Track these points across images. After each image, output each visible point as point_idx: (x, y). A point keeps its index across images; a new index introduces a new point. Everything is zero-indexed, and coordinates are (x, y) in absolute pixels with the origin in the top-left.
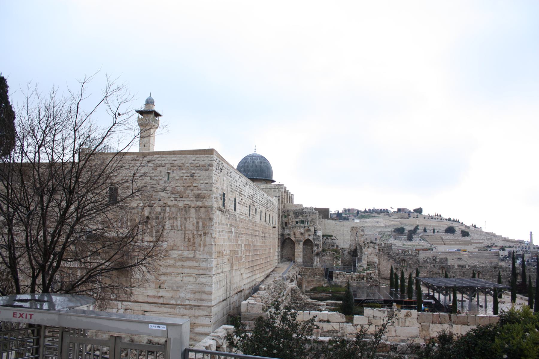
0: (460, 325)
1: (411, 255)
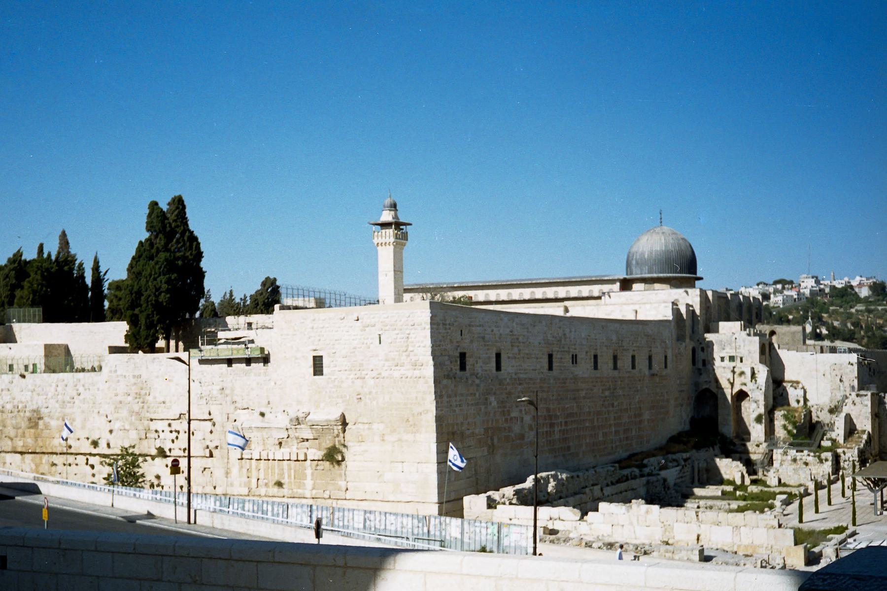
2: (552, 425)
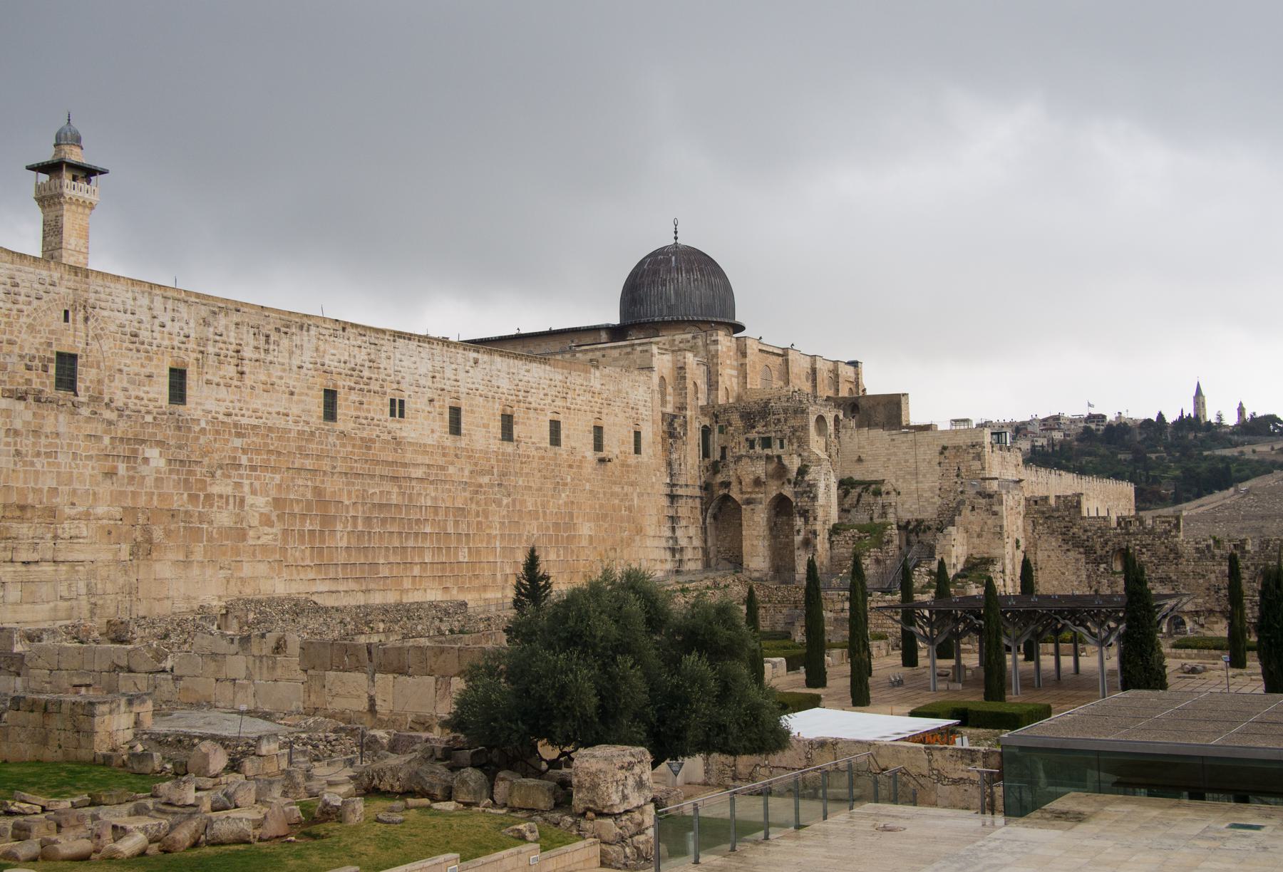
0: (390, 676)
1: (1151, 532)
2: (327, 520)
